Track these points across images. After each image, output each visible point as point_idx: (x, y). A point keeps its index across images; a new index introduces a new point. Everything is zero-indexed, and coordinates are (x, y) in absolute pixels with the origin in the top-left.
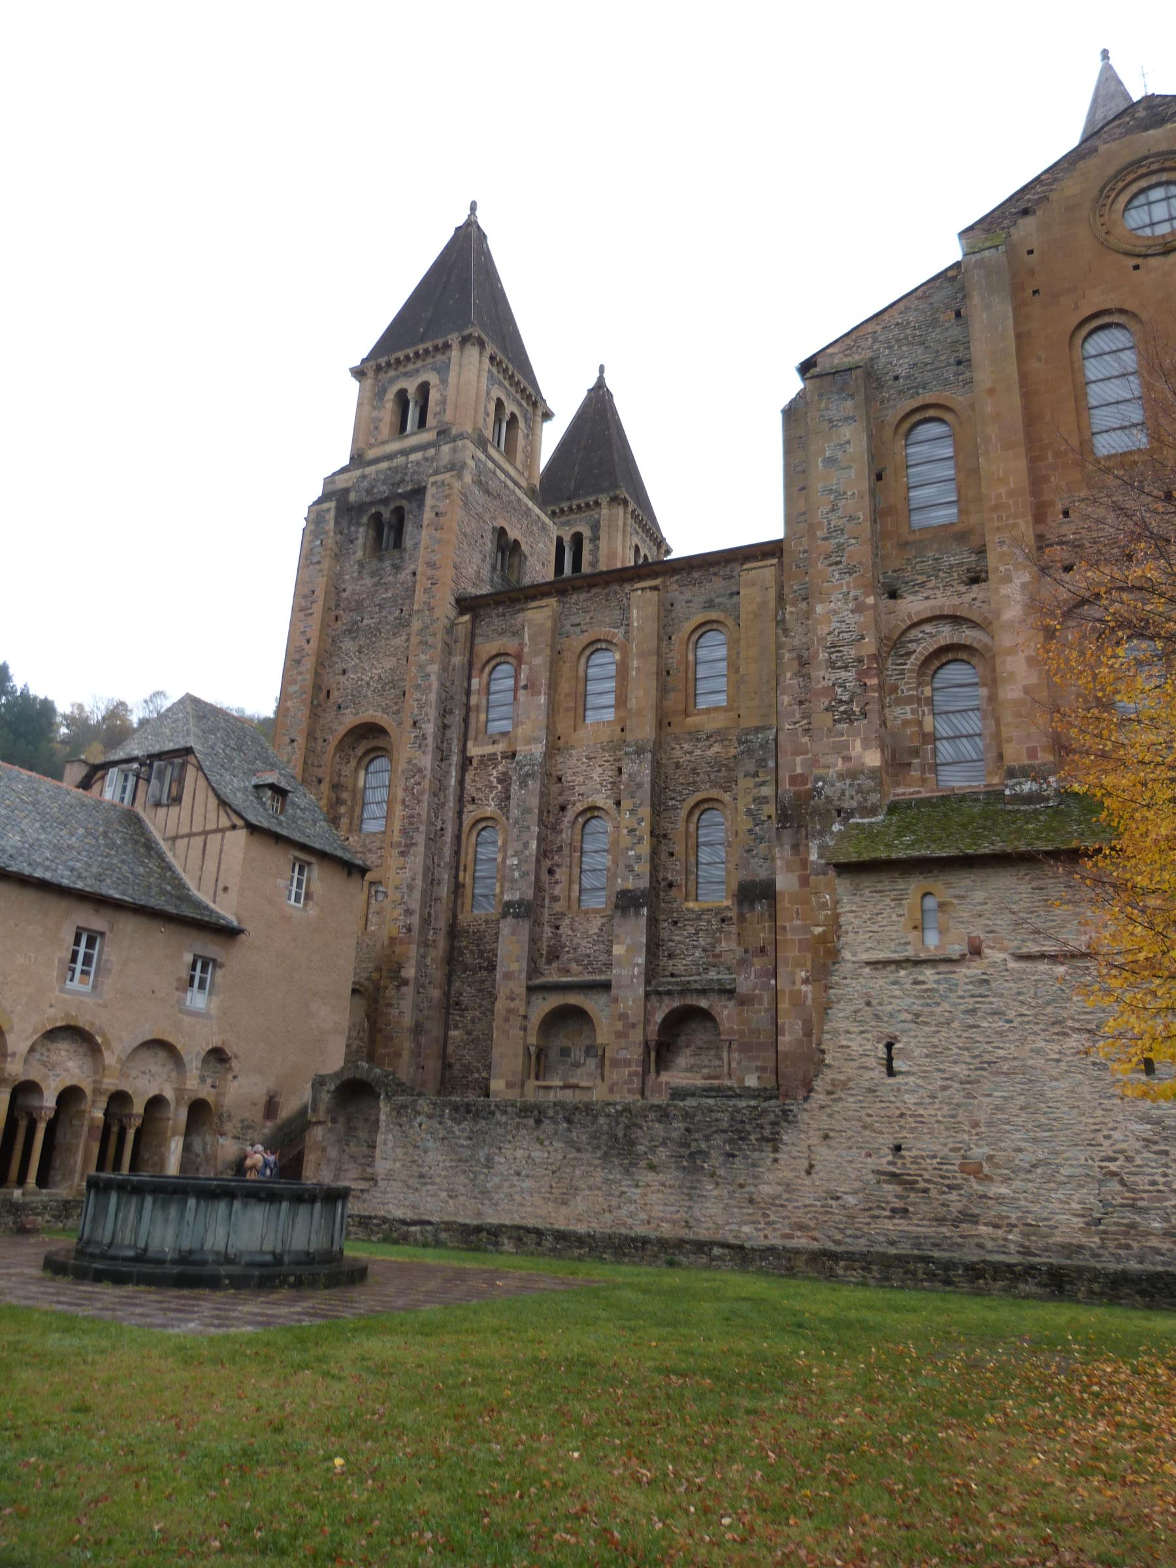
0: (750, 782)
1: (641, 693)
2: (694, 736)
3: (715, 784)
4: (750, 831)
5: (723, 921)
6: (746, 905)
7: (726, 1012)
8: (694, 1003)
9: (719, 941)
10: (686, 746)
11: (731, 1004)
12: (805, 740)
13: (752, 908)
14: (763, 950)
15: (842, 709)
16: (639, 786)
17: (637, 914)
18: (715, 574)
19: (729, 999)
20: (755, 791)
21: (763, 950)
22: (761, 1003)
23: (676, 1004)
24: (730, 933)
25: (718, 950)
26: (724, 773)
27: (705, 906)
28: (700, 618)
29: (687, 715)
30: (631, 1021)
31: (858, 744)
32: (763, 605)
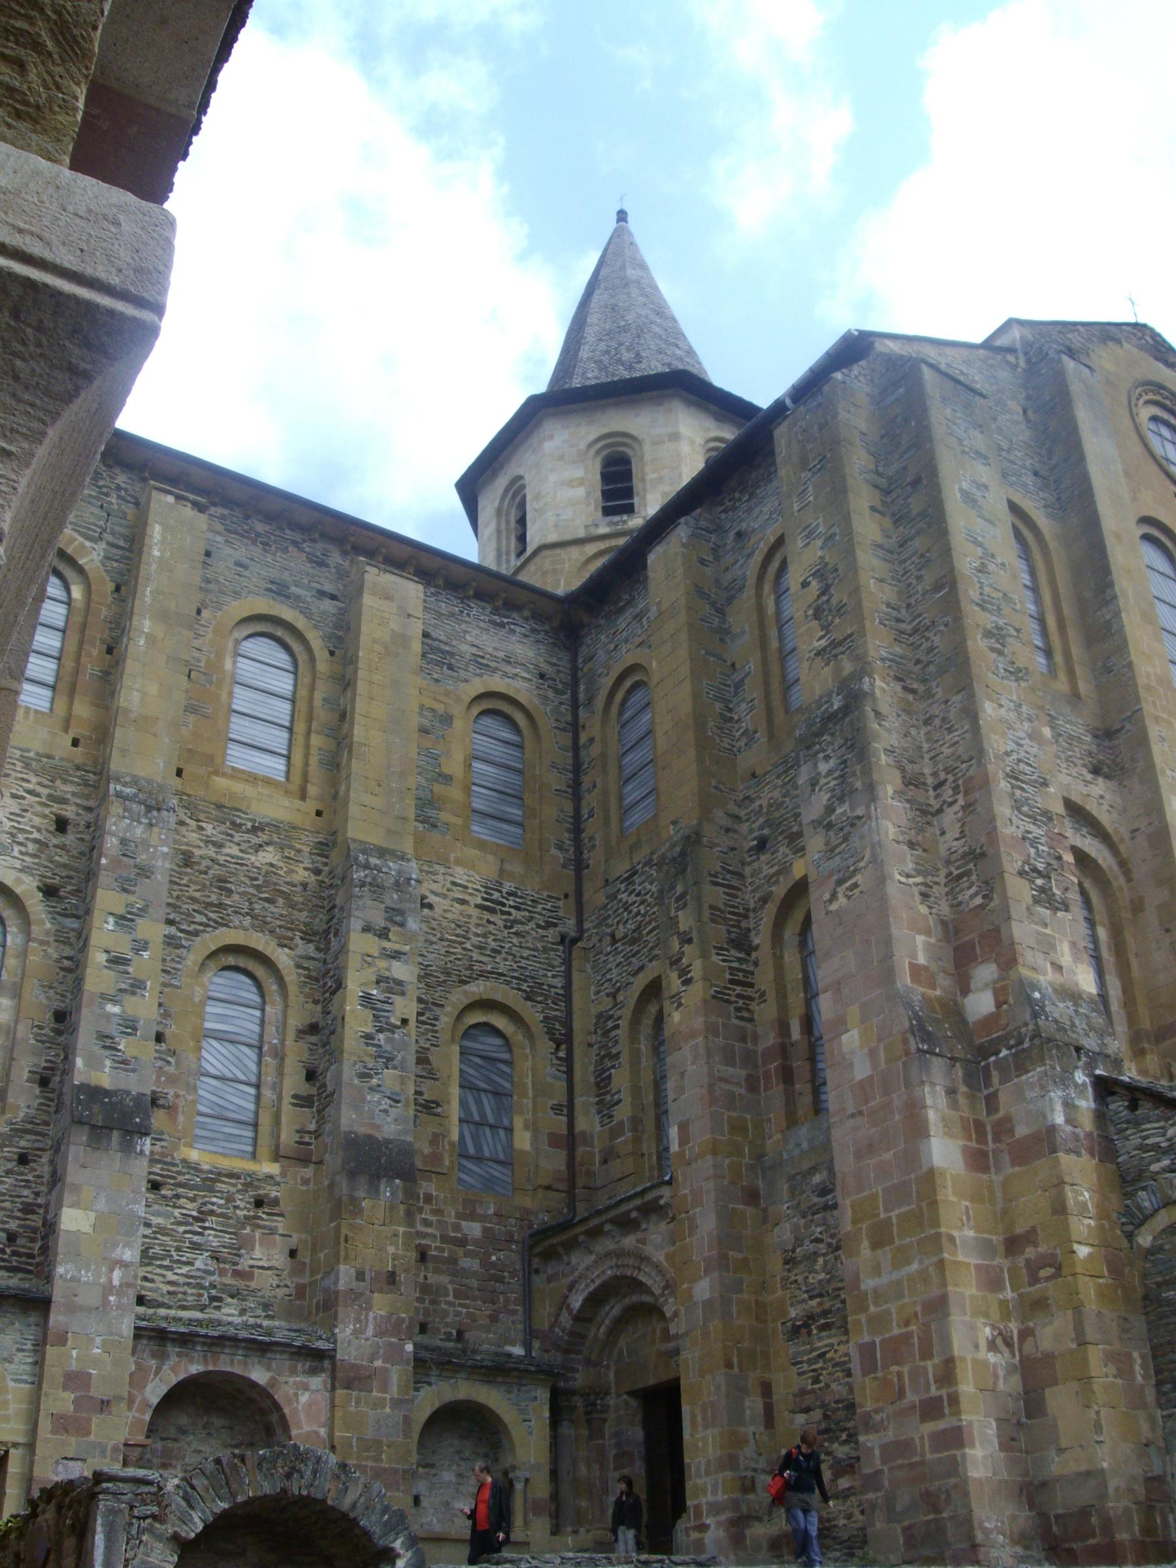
1: (153, 689)
2: (228, 815)
3: (262, 924)
4: (368, 1037)
5: (259, 1203)
6: (363, 1179)
7: (304, 1398)
8: (238, 1370)
10: (209, 828)
11: (317, 1382)
13: (374, 1191)
14: (392, 1278)
16: (145, 872)
17: (127, 1148)
18: (296, 544)
19: (313, 1372)
20: (382, 964)
21: (392, 1278)
22: (384, 1388)
23: (195, 1369)
24: (273, 1231)
26: (280, 907)
27: (226, 1164)
28: (262, 605)
29: (216, 773)
30: (98, 1391)
32: (401, 639)
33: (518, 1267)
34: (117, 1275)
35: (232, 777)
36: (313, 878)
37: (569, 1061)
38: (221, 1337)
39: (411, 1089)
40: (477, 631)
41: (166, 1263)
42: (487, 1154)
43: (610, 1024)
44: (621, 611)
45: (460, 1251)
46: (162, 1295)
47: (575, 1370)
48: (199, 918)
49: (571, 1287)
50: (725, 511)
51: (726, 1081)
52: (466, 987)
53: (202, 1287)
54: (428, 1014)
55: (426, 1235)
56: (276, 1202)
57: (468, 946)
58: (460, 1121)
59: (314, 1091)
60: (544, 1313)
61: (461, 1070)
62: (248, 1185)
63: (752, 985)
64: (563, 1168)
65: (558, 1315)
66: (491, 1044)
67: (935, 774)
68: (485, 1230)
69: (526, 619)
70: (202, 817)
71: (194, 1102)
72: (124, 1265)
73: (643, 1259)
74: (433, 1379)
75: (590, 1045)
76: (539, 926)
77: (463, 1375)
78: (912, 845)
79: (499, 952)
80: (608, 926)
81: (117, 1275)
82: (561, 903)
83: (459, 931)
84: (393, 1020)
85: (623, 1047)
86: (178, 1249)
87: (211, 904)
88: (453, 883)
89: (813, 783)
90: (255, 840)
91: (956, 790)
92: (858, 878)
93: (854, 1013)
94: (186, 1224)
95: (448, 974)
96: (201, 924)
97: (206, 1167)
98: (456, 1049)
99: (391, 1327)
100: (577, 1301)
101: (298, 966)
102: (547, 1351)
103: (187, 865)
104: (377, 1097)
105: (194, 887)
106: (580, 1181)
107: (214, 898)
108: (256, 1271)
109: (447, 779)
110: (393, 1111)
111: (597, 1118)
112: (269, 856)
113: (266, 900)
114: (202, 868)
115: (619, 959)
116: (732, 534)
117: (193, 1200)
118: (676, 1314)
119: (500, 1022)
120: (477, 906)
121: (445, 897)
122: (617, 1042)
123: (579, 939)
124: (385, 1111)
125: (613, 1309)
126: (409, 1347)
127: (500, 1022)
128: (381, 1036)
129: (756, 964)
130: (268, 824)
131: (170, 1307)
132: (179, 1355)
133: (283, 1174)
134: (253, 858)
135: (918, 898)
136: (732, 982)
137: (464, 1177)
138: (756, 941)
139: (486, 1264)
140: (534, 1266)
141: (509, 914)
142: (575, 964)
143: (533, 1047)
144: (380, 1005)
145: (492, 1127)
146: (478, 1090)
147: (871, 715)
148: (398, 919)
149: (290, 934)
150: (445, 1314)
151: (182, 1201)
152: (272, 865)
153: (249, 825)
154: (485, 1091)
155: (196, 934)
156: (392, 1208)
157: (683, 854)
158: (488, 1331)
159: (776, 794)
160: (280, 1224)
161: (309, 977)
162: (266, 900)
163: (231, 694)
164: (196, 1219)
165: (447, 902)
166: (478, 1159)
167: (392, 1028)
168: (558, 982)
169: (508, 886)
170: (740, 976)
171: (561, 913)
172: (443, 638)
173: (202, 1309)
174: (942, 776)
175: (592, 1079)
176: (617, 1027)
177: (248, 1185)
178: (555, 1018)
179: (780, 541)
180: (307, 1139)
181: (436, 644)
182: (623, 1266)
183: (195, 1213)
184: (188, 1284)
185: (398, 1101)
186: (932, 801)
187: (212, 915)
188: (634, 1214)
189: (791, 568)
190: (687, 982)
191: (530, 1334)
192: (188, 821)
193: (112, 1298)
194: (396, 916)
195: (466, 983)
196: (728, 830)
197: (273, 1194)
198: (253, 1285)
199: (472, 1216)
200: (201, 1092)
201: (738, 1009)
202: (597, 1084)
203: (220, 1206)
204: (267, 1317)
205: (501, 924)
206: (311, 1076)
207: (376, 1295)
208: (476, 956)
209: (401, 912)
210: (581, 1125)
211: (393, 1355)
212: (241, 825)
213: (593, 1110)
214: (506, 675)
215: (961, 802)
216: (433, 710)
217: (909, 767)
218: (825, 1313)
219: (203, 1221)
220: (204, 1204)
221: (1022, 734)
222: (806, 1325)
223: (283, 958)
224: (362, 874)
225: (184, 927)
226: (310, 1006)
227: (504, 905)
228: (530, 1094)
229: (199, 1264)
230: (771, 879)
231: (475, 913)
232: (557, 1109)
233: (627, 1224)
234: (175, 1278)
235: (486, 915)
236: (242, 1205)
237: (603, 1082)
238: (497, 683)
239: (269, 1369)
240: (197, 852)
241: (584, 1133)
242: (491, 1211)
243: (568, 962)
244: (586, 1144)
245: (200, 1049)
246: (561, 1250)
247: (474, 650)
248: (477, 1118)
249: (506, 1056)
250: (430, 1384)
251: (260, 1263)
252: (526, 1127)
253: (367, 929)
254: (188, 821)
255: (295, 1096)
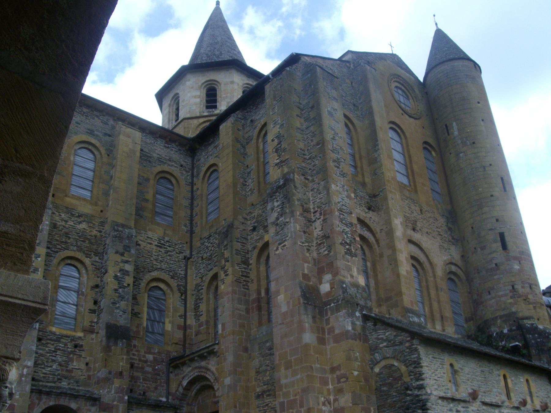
0: (119, 258)
2: (70, 210)
3: (80, 249)
4: (116, 290)
5: (76, 346)
9: (72, 360)
10: (63, 215)
12: (308, 255)
13: (116, 344)
14: (121, 373)
15: (347, 247)
18: (97, 116)
19: (93, 405)
20: (122, 265)
23: (51, 403)
25: (70, 367)
26: (87, 244)
27: (65, 332)
28: (85, 138)
29: (66, 196)
31: (355, 270)
33: (165, 371)
34: (25, 371)
35: (72, 198)
36: (99, 234)
37: (185, 300)
38: (61, 393)
39: (130, 309)
40: (160, 149)
41: (43, 366)
42: (156, 331)
43: (200, 288)
44: (210, 144)
45: (145, 365)
46: (41, 378)
47: (183, 407)
48: (59, 247)
49: (183, 378)
50: (247, 112)
51: (239, 310)
52: (151, 273)
53: (54, 375)
54: (137, 282)
55: (134, 359)
56: (82, 346)
57: (152, 259)
58: (147, 319)
59: (96, 308)
60: (173, 387)
61: (148, 302)
62: (72, 340)
63: (249, 277)
64: (182, 337)
65: (178, 388)
66: (158, 293)
67: (314, 208)
68: (154, 358)
69: (177, 146)
70: (61, 211)
71: (55, 311)
72: (28, 367)
73: (208, 370)
74: (134, 409)
75: (193, 295)
76: (177, 253)
77: (145, 407)
78: (305, 232)
79: (162, 262)
80: (201, 254)
81: (25, 371)
82: (185, 245)
83: (149, 254)
84: (125, 284)
85: (204, 296)
86: (47, 362)
87: (63, 242)
88: (148, 237)
89: (272, 209)
90: (79, 220)
91: (321, 214)
92: (286, 243)
93: (282, 289)
94: (50, 353)
95: (144, 268)
96: (59, 249)
97: (58, 333)
98: (146, 295)
99: (120, 390)
100: (185, 383)
101: (92, 264)
102: (174, 400)
103: (54, 228)
104: (118, 311)
105: (57, 236)
106: (188, 342)
107: (64, 240)
108: (74, 370)
109: (147, 201)
110: (124, 316)
111: (194, 320)
112: (84, 226)
113: (82, 241)
114: (60, 229)
115: (204, 265)
116: (249, 120)
117: (53, 345)
118: (218, 389)
119: (162, 286)
120: (155, 245)
121: (145, 242)
122: (202, 294)
123: (190, 258)
124: (121, 316)
125: (197, 387)
126: (126, 398)
127: (162, 286)
128: (120, 290)
129: (250, 270)
130: (83, 215)
131: (43, 382)
132: (46, 399)
133: (85, 336)
134: (78, 226)
135: (306, 251)
136: (242, 276)
137: (147, 339)
138: (251, 262)
139: (154, 369)
140: (171, 371)
141: (167, 248)
142: (189, 267)
143: (173, 295)
144: (120, 279)
145: (158, 322)
146: (154, 309)
147: (293, 187)
148: (128, 249)
149: (90, 253)
150: (139, 386)
151: (49, 345)
152: (84, 229)
153: (77, 214)
154: (156, 309)
155: (57, 252)
156: (122, 349)
157: (227, 231)
158: (154, 393)
159: (260, 212)
160: (83, 354)
161: (96, 268)
162: (82, 241)
163: (72, 168)
164: (54, 351)
165: (145, 244)
166: (153, 333)
167: (124, 287)
168: (183, 273)
169: (167, 239)
170: (245, 274)
171: (185, 249)
172: (147, 151)
173: (55, 382)
174: (316, 209)
175: (193, 307)
176: (202, 289)
177: (72, 340)
178: (181, 285)
179: (265, 124)
180: (93, 325)
181: (145, 153)
182: (201, 372)
183: (53, 349)
184: (50, 374)
185: (125, 313)
186: (312, 217)
187: (63, 246)
188: (205, 354)
189: (269, 134)
190: (227, 275)
191: (168, 394)
192: (56, 213)
193: (23, 379)
194: (127, 248)
195: (150, 272)
196: (243, 223)
197: (81, 343)
198: (73, 374)
199: (150, 353)
200: (57, 307)
201: (244, 285)
202: (195, 309)
203: (62, 347)
204: (78, 386)
205: (163, 251)
206: (95, 303)
207: (115, 379)
208: (154, 263)
209: (129, 247)
210: (189, 322)
211: (121, 400)
212: (74, 215)
213: (193, 317)
214: (169, 165)
215: (322, 218)
216: (143, 177)
217: (305, 206)
218: (269, 391)
219: (56, 352)
220: (57, 346)
221: (344, 196)
222: (262, 394)
223: (87, 261)
224: (116, 233)
225: (53, 249)
226: (96, 278)
227: (165, 245)
228: (172, 311)
229: (54, 367)
230: (257, 241)
231: (155, 248)
232: (180, 316)
233: (203, 357)
234: (45, 372)
235: (159, 249)
236: (70, 347)
237: (197, 308)
238: (166, 168)
239: (77, 404)
240: (58, 224)
241: (189, 325)
242: (156, 351)
243: (186, 266)
244: (190, 328)
245: (57, 292)
246: (180, 365)
247: (158, 156)
248: (153, 319)
249: (163, 298)
250: (133, 410)
251: (76, 367)
252: (170, 322)
253: (117, 252)
254: (56, 213)
255: (89, 310)
